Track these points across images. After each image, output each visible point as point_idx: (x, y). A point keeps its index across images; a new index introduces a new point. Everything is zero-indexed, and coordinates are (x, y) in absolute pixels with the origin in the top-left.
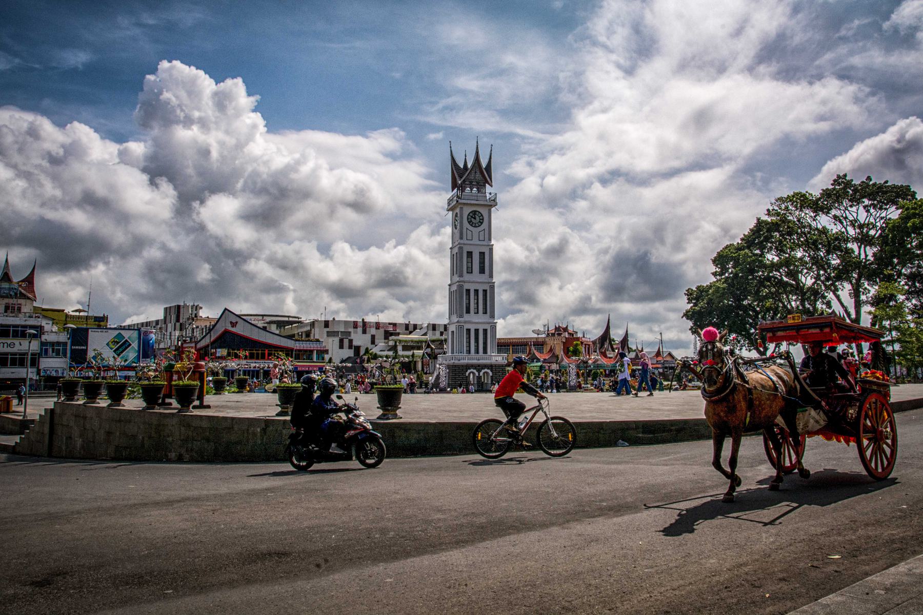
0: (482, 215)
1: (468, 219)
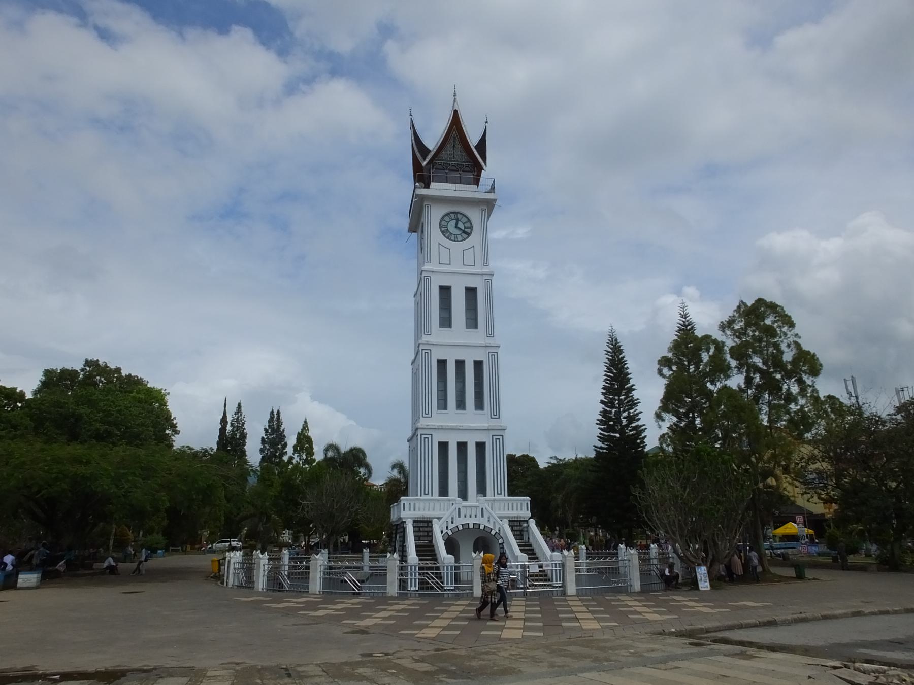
0: (469, 221)
1: (441, 227)
